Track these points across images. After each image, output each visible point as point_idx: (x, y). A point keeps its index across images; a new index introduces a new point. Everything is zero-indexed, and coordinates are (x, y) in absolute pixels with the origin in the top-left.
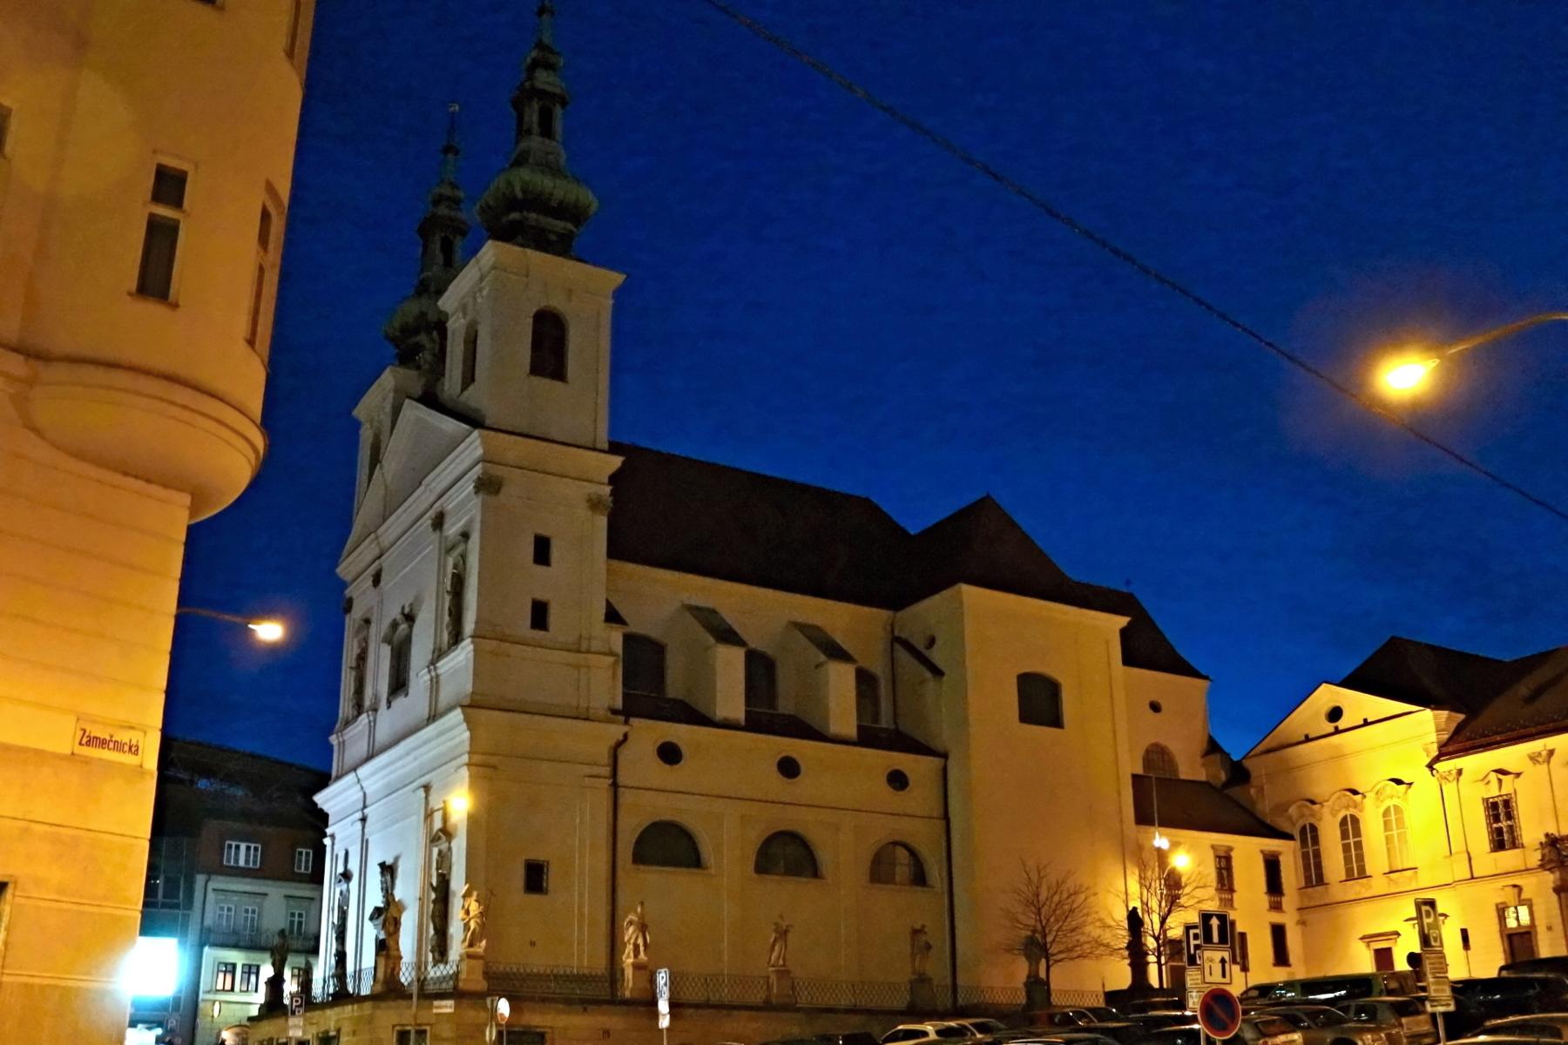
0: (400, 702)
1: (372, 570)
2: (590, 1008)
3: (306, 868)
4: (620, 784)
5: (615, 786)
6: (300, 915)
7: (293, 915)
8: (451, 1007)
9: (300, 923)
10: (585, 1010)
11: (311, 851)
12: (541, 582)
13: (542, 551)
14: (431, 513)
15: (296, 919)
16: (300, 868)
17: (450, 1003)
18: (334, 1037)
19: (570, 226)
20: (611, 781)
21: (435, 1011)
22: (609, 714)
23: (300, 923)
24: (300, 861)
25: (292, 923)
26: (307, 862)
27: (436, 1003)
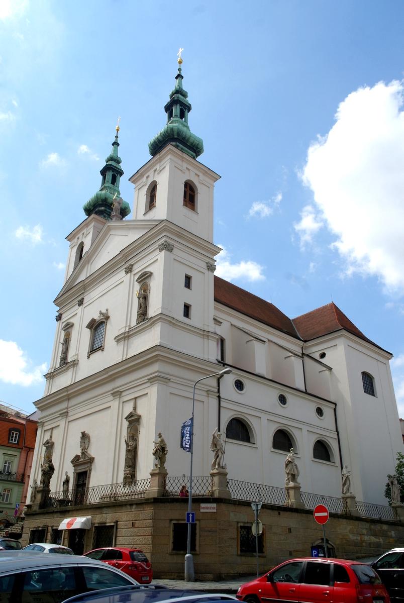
0: (97, 355)
1: (80, 298)
2: (282, 513)
3: (15, 440)
4: (221, 397)
5: (219, 397)
7: (6, 463)
8: (214, 508)
9: (9, 467)
10: (279, 514)
12: (187, 296)
13: (188, 281)
14: (125, 266)
15: (7, 465)
16: (12, 440)
17: (215, 505)
18: (113, 526)
19: (195, 154)
20: (218, 395)
21: (202, 511)
22: (217, 362)
23: (9, 467)
24: (13, 437)
25: (5, 466)
26: (16, 437)
27: (202, 505)
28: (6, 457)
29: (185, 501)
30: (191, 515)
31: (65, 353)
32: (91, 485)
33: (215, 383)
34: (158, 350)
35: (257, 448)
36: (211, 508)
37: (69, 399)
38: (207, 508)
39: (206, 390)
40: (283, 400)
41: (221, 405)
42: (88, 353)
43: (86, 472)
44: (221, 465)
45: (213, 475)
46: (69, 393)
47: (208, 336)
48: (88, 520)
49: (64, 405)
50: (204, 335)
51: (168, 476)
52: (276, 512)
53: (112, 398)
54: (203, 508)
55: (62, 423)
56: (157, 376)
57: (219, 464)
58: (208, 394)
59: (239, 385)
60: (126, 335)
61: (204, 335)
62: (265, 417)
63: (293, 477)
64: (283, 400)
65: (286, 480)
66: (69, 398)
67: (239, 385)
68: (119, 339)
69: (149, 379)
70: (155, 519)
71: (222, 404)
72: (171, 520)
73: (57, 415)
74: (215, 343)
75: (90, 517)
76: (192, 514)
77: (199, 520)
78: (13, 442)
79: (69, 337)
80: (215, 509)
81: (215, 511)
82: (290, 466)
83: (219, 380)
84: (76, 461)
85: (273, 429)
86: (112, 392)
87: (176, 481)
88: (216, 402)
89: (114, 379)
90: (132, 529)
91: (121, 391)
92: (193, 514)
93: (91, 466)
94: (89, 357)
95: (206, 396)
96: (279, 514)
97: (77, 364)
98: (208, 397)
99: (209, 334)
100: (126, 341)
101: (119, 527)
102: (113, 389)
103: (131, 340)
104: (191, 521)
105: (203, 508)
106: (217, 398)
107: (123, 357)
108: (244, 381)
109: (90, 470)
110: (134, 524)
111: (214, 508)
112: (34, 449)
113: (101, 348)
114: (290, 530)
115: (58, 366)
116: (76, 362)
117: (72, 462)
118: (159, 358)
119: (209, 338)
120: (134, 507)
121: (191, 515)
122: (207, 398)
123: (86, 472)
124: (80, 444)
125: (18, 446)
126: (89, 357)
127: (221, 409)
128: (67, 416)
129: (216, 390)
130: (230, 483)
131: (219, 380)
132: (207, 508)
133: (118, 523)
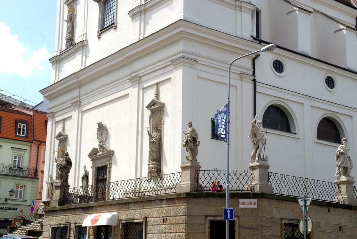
0: (109, 34)
3: (23, 134)
4: (257, 81)
5: (254, 80)
6: (19, 158)
8: (255, 204)
10: (329, 210)
11: (26, 125)
16: (19, 133)
17: (255, 201)
20: (253, 78)
21: (241, 206)
22: (251, 39)
24: (20, 129)
26: (23, 130)
27: (242, 201)
28: (15, 151)
29: (223, 196)
30: (229, 211)
31: (71, 31)
32: (112, 180)
33: (249, 65)
34: (181, 26)
35: (299, 138)
36: (252, 203)
37: (80, 87)
38: (246, 204)
39: (239, 73)
40: (330, 82)
41: (257, 90)
42: (98, 32)
43: (105, 167)
44: (262, 157)
45: (253, 168)
46: (80, 79)
47: (241, 7)
48: (113, 216)
49: (75, 93)
50: (236, 6)
51: (201, 169)
52: (326, 209)
53: (129, 84)
54: (242, 204)
55: (75, 114)
56: (182, 57)
57: (259, 156)
58: (242, 78)
59: (278, 66)
60: (143, 8)
61: (236, 6)
62: (308, 103)
63: (346, 171)
64: (330, 82)
65: (337, 174)
66: (80, 85)
67: (278, 66)
68: (134, 14)
69: (172, 61)
70: (189, 215)
71: (258, 89)
72: (206, 216)
73: (68, 104)
74: (249, 16)
75: (115, 213)
76: (230, 210)
77: (238, 217)
78: (21, 135)
79: (73, 13)
80: (256, 205)
81: (256, 206)
82: (341, 158)
83: (254, 60)
84: (93, 155)
85: (318, 116)
86: (130, 77)
87: (243, 175)
88: (251, 86)
89: (131, 62)
90: (163, 226)
91: (140, 75)
92: (231, 210)
93: (110, 160)
94: (99, 37)
95: (239, 80)
96: (329, 210)
97: (87, 45)
98: (242, 80)
99: (242, 5)
100: (143, 16)
101: (149, 223)
102: (131, 74)
103: (148, 14)
104: (229, 217)
105: (242, 204)
106: (252, 82)
107: (140, 35)
108: (285, 62)
109: (111, 165)
110: (165, 221)
111: (255, 204)
112: (45, 142)
113: (114, 25)
114: (341, 228)
115: (64, 48)
116: (85, 43)
117: (90, 156)
118: (183, 35)
119: (243, 9)
120: (164, 202)
121: (229, 211)
122: (240, 82)
123: (105, 167)
124: (96, 136)
125: (26, 139)
126: (99, 37)
127: (257, 95)
128: (80, 106)
129: (251, 73)
130: (273, 177)
131: (254, 60)
132: (246, 204)
133: (147, 219)
